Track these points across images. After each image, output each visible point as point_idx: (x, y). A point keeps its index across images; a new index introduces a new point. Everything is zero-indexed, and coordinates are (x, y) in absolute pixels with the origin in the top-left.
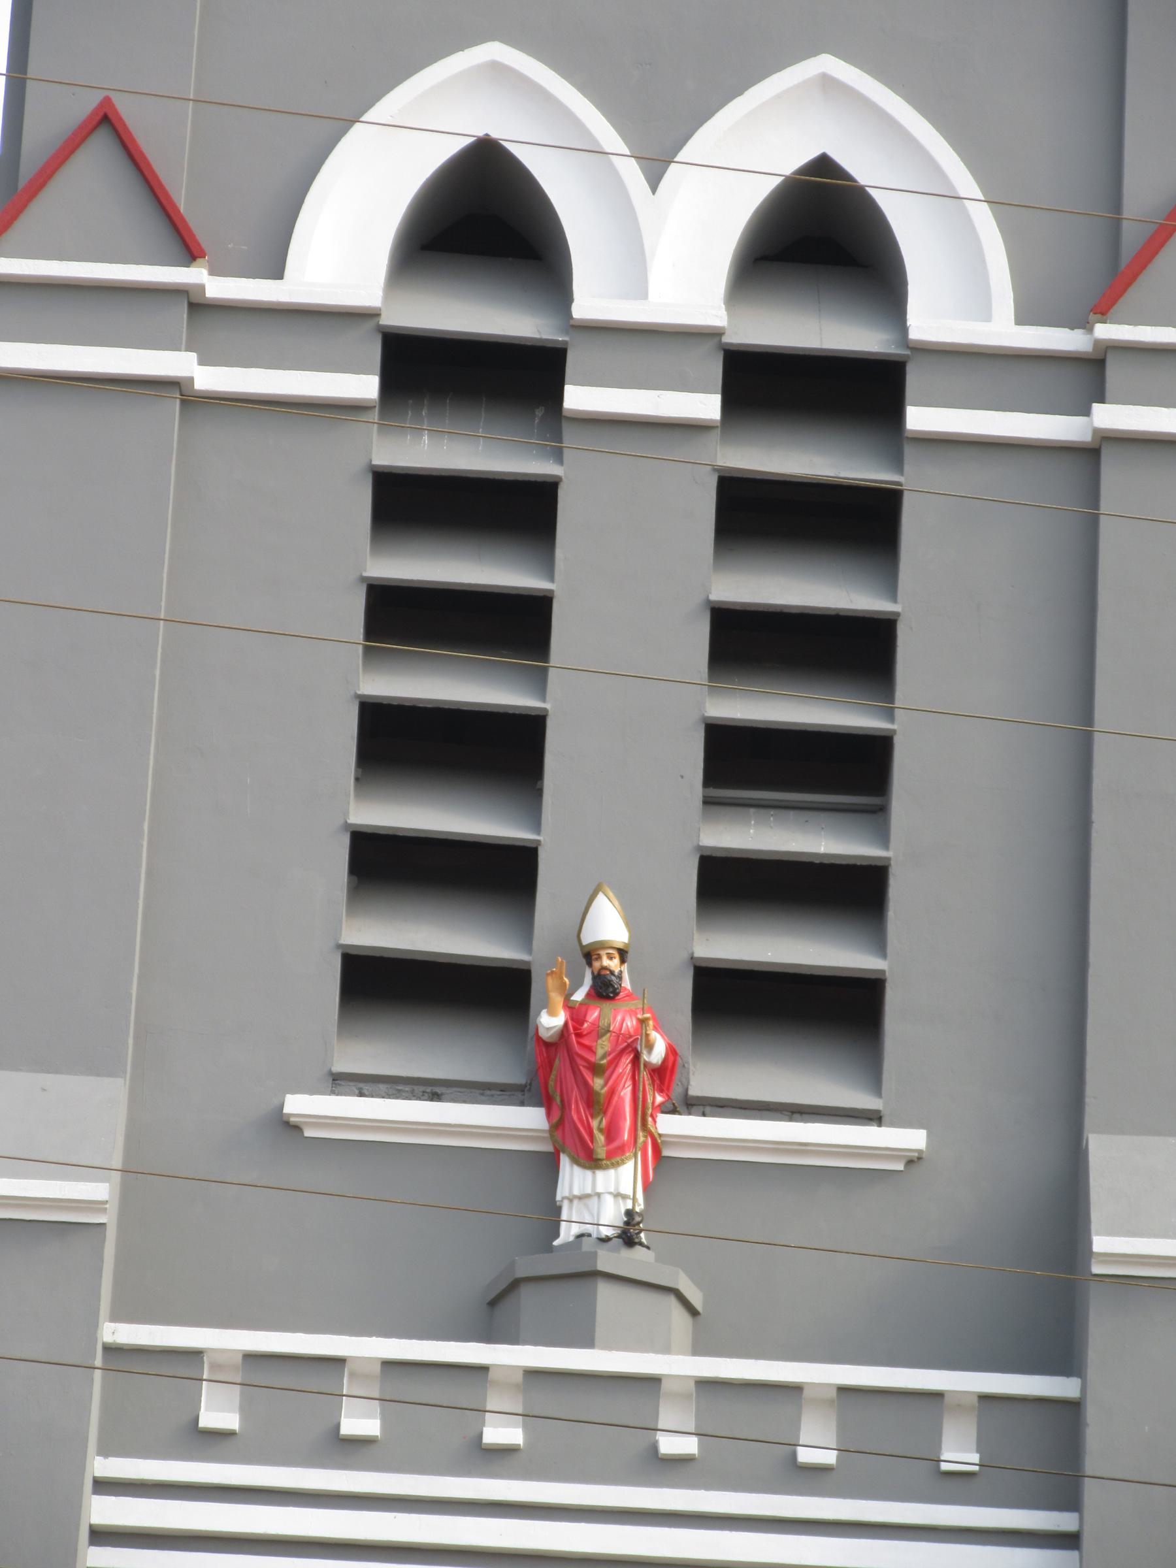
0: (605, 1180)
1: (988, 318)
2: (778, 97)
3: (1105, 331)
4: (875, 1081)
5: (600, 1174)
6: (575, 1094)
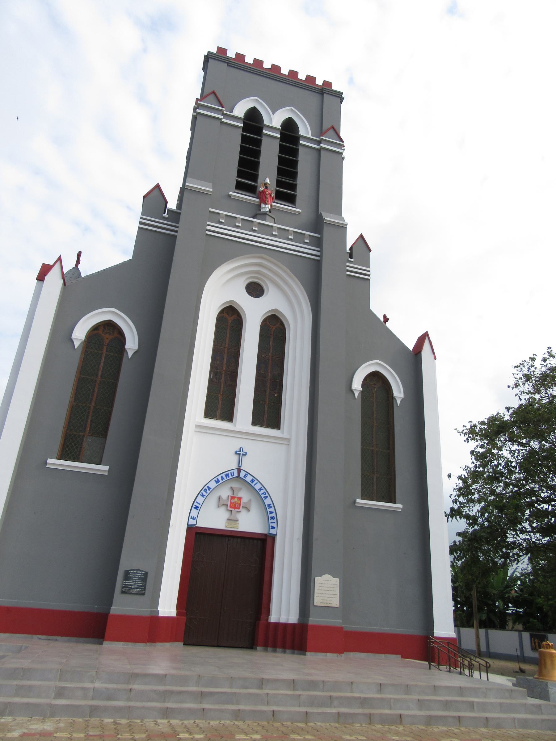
0: (267, 206)
1: (308, 134)
2: (287, 110)
3: (321, 137)
4: (295, 206)
5: (266, 205)
6: (264, 197)
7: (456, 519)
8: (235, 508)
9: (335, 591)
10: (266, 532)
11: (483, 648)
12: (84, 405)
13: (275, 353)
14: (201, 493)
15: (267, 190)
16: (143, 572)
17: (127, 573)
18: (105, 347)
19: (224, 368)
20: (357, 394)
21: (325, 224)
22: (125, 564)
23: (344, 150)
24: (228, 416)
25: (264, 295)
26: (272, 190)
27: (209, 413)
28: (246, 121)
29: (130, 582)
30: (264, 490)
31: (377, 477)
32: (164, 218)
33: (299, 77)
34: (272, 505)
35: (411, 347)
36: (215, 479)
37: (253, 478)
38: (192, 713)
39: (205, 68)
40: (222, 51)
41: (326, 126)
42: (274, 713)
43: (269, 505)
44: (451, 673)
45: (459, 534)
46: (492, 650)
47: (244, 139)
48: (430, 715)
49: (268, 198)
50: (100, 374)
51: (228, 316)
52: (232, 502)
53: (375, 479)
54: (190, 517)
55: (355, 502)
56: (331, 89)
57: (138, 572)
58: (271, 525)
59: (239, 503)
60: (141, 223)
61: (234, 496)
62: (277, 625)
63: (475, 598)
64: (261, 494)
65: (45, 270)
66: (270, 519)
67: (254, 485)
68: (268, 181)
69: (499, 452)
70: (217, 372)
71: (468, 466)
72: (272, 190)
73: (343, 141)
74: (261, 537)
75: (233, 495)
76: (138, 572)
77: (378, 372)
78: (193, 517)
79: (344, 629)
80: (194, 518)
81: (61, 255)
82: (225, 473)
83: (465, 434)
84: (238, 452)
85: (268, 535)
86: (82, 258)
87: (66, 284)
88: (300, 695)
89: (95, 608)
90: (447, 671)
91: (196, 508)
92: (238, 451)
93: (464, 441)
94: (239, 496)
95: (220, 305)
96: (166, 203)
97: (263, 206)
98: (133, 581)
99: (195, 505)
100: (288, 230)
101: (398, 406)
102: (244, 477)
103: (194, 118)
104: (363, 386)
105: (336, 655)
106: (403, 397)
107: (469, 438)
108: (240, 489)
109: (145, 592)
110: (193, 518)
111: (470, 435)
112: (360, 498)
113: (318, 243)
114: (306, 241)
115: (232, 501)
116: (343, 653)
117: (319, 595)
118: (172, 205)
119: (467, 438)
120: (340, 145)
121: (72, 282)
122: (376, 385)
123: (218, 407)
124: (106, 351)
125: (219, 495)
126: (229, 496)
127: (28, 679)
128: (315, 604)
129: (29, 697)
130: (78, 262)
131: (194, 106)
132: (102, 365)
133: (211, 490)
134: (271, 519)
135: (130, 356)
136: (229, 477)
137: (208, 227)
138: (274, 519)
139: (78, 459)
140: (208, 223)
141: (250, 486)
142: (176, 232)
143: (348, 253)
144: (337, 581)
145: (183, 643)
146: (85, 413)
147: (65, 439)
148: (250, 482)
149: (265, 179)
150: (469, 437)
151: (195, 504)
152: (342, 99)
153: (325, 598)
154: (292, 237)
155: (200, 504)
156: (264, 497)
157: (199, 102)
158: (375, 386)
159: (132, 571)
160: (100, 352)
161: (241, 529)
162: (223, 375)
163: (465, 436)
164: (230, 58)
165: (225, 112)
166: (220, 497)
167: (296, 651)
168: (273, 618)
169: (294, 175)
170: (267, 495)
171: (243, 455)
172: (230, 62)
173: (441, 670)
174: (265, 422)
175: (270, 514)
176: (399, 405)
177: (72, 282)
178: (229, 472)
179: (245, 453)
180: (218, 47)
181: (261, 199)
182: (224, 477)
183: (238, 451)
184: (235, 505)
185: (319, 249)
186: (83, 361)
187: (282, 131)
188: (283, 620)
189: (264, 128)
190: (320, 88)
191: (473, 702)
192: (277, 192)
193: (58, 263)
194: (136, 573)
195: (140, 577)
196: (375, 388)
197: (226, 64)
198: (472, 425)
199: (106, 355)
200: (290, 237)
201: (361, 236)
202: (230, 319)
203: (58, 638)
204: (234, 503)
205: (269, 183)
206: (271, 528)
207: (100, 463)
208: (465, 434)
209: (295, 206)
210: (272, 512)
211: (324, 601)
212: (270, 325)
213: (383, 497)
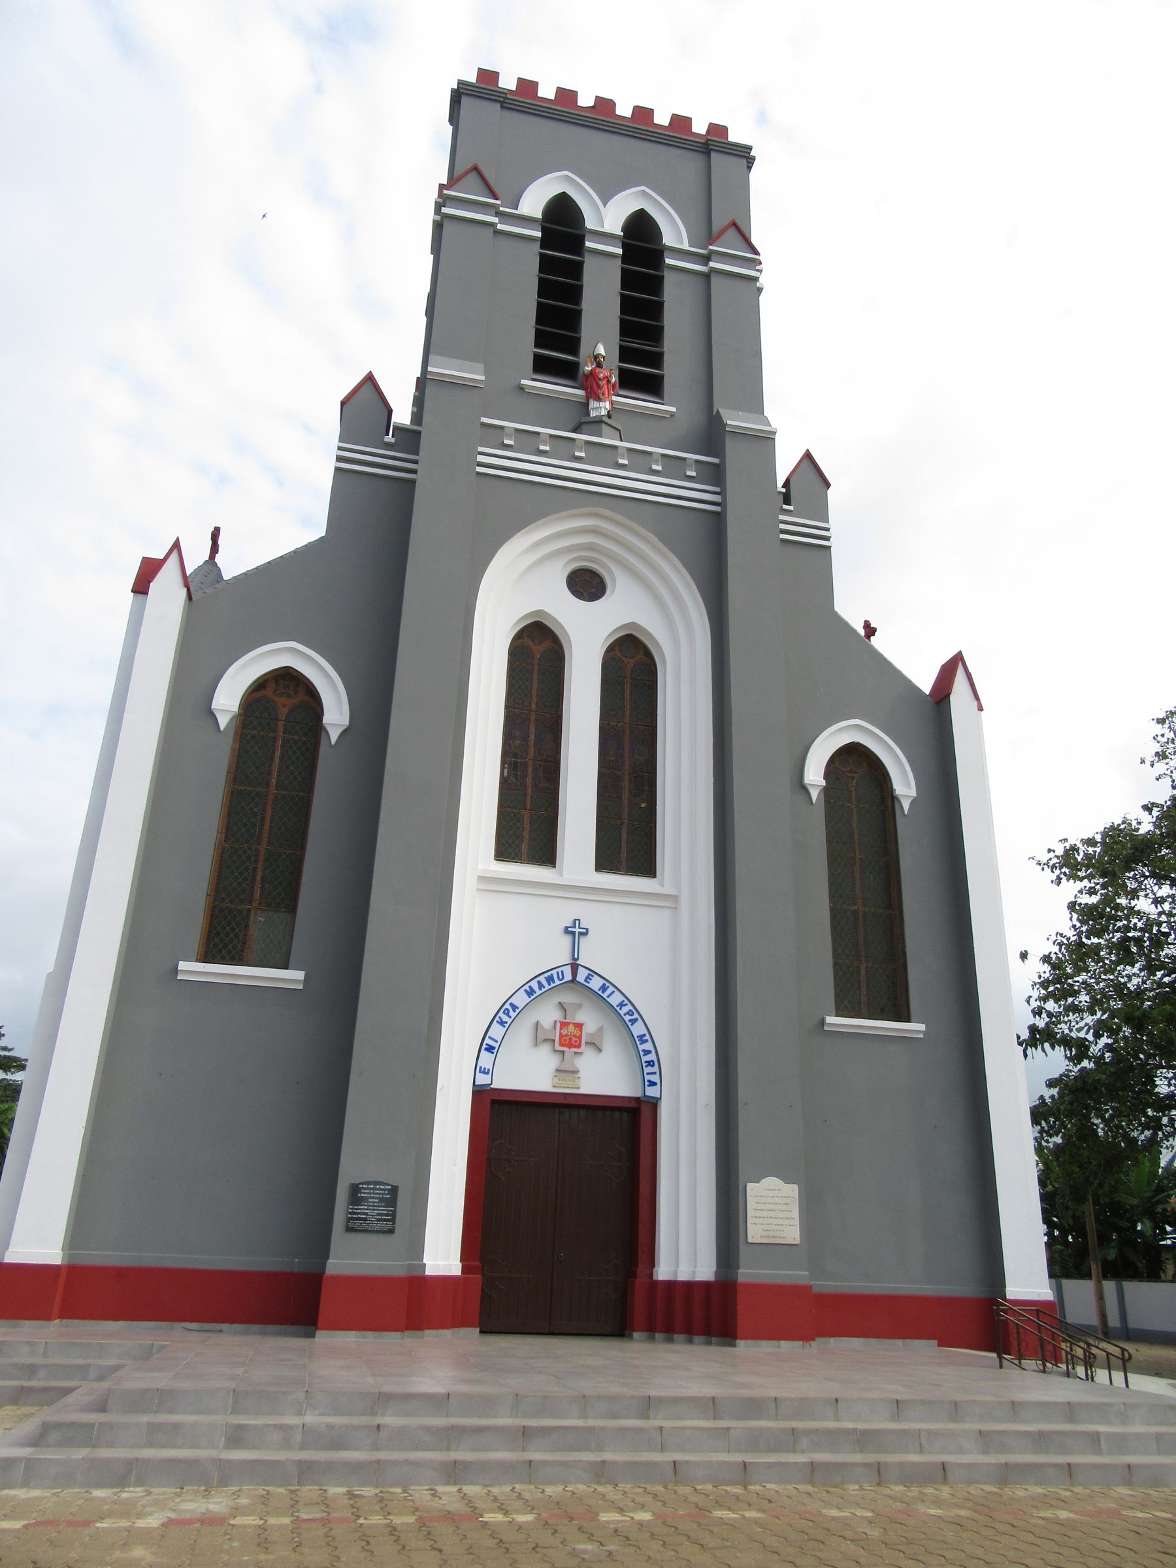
0: (602, 404)
3: (711, 247)
4: (662, 399)
7: (1043, 1050)
8: (570, 1046)
9: (791, 1211)
10: (638, 1094)
11: (1114, 1321)
12: (246, 846)
13: (637, 716)
14: (497, 1019)
15: (601, 370)
16: (387, 1187)
17: (355, 1190)
18: (281, 724)
19: (531, 754)
20: (814, 794)
21: (727, 434)
22: (350, 1171)
23: (760, 271)
24: (546, 854)
25: (605, 596)
26: (611, 370)
27: (506, 850)
28: (545, 224)
29: (362, 1207)
30: (629, 1007)
31: (867, 967)
32: (388, 446)
33: (695, 130)
34: (647, 1037)
35: (926, 687)
36: (526, 987)
37: (605, 982)
38: (507, 1470)
39: (454, 118)
40: (488, 77)
41: (718, 223)
42: (676, 1467)
43: (641, 1037)
44: (1045, 1375)
45: (1051, 1084)
46: (1133, 1324)
47: (546, 264)
48: (1006, 1464)
49: (603, 386)
50: (274, 781)
51: (532, 643)
52: (564, 1034)
53: (863, 972)
54: (478, 1069)
55: (822, 1022)
56: (726, 141)
57: (378, 1187)
58: (647, 1077)
59: (578, 1035)
60: (339, 459)
61: (566, 1021)
62: (671, 1285)
63: (1091, 1215)
64: (623, 1016)
65: (148, 571)
66: (644, 1067)
67: (608, 997)
68: (601, 350)
69: (1130, 904)
70: (515, 763)
71: (1062, 934)
72: (611, 370)
73: (757, 253)
74: (626, 1104)
75: (565, 1019)
76: (378, 1187)
77: (859, 744)
78: (485, 1069)
79: (815, 1290)
80: (486, 1071)
81: (178, 538)
82: (546, 975)
83: (1053, 867)
84: (570, 929)
85: (642, 1099)
86: (221, 541)
87: (193, 596)
88: (728, 1429)
89: (295, 1264)
90: (1038, 1372)
91: (490, 1049)
92: (570, 927)
93: (1052, 882)
94: (579, 1019)
95: (515, 621)
96: (390, 412)
97: (593, 404)
98: (369, 1206)
99: (487, 1044)
100: (650, 453)
101: (905, 815)
102: (586, 981)
103: (438, 228)
104: (827, 775)
105: (799, 1343)
106: (915, 795)
107: (1062, 876)
108: (580, 1006)
109: (394, 1228)
110: (485, 1072)
111: (1064, 870)
112: (834, 1014)
113: (715, 475)
114: (689, 473)
115: (564, 1032)
116: (814, 1339)
117: (757, 1221)
118: (402, 415)
119: (1058, 876)
120: (751, 260)
121: (205, 593)
122: (856, 772)
123: (523, 836)
124: (284, 733)
125: (536, 1021)
126: (555, 1022)
127: (171, 1411)
128: (750, 1240)
129: (173, 1447)
130: (215, 549)
131: (436, 202)
132: (277, 761)
133: (518, 1011)
134: (646, 1066)
135: (333, 740)
136: (554, 982)
137: (480, 458)
138: (653, 1066)
139: (241, 960)
140: (481, 449)
141: (598, 998)
142: (414, 472)
143: (780, 493)
144: (792, 1190)
145: (478, 1329)
146: (248, 864)
147: (211, 919)
148: (599, 990)
149: (596, 346)
150: (1061, 873)
151: (487, 1041)
152: (750, 161)
153: (769, 1227)
154: (659, 468)
155: (497, 1042)
156: (630, 1021)
157: (445, 192)
158: (854, 775)
159: (364, 1186)
160: (271, 735)
161: (584, 1090)
162: (530, 769)
163: (1053, 872)
164: (506, 91)
165: (501, 209)
166: (537, 1025)
167: (714, 1339)
168: (663, 1272)
169: (656, 334)
170: (636, 1016)
171: (581, 934)
172: (506, 101)
173: (1024, 1369)
174: (624, 863)
175: (644, 1055)
176: (906, 813)
177: (205, 593)
178: (554, 972)
179: (585, 931)
180: (479, 69)
181: (589, 390)
182: (544, 982)
183: (570, 927)
184: (570, 1039)
185: (718, 489)
186: (238, 756)
187: (625, 240)
188: (683, 1275)
189: (586, 237)
190: (703, 141)
191: (1098, 1432)
192: (623, 373)
193: (175, 554)
194: (375, 1189)
195: (381, 1196)
196: (853, 778)
197: (499, 105)
198: (1068, 848)
199: (285, 741)
200: (654, 467)
201: (808, 456)
202: (538, 649)
203: (225, 1326)
204: (567, 1035)
205: (603, 353)
206: (648, 1086)
207: (285, 966)
208: (1053, 867)
209: (662, 399)
210: (648, 1052)
211: (767, 1233)
212: (623, 658)
213: (882, 1010)
